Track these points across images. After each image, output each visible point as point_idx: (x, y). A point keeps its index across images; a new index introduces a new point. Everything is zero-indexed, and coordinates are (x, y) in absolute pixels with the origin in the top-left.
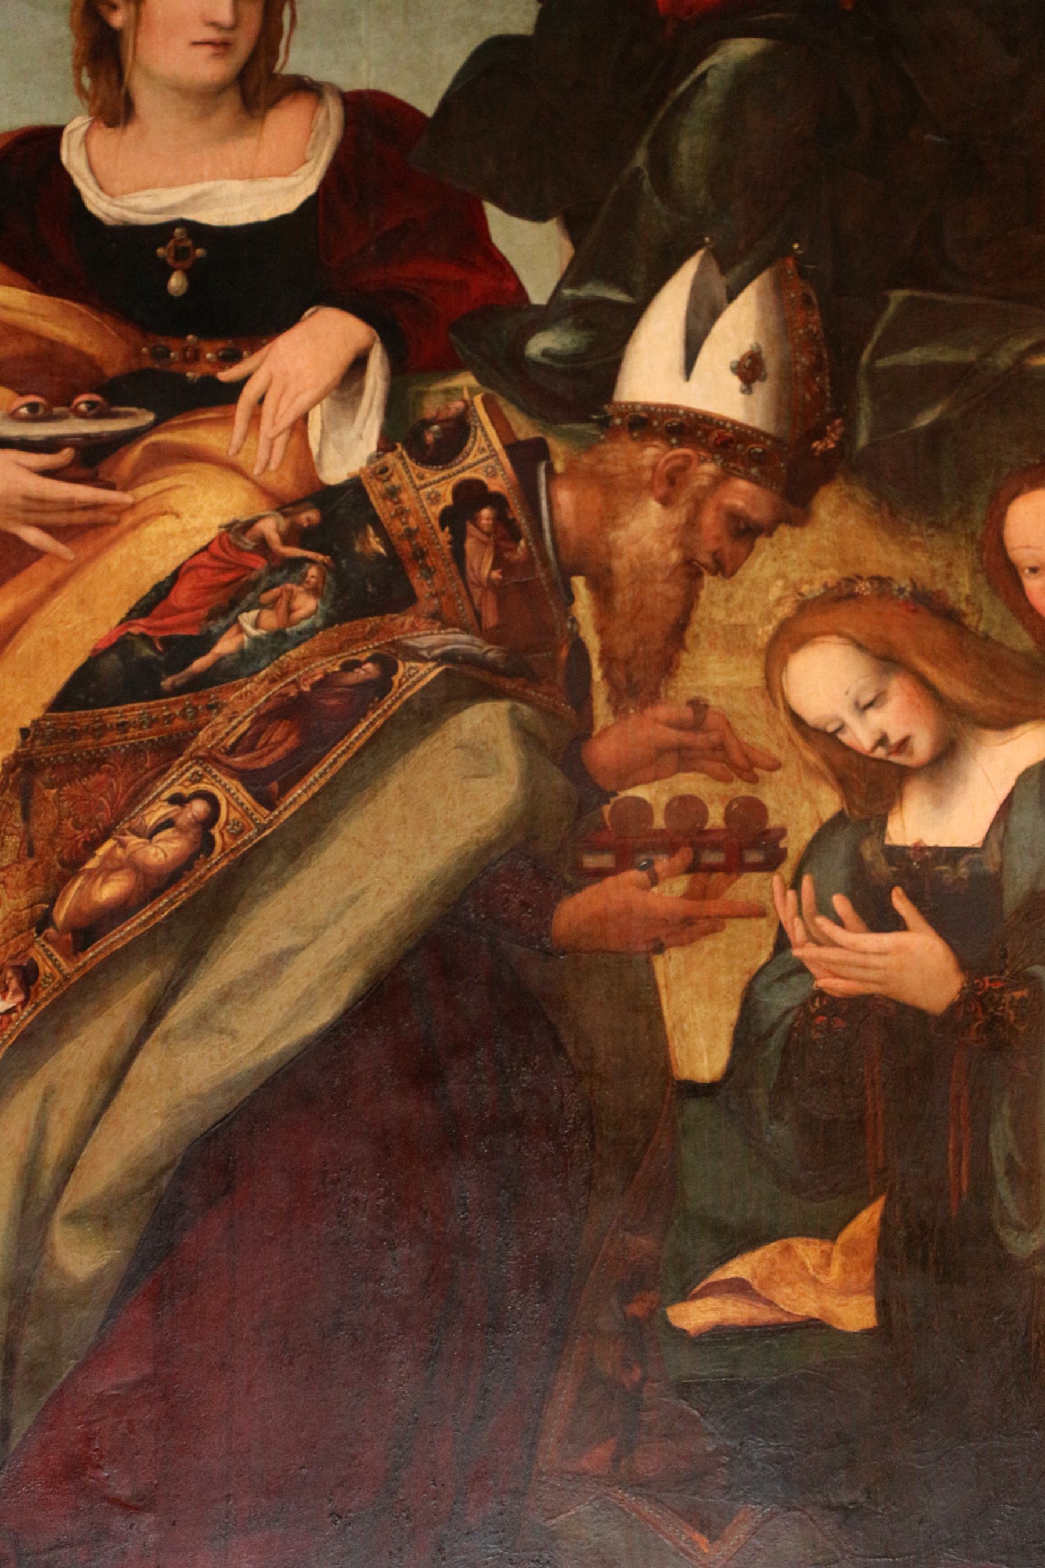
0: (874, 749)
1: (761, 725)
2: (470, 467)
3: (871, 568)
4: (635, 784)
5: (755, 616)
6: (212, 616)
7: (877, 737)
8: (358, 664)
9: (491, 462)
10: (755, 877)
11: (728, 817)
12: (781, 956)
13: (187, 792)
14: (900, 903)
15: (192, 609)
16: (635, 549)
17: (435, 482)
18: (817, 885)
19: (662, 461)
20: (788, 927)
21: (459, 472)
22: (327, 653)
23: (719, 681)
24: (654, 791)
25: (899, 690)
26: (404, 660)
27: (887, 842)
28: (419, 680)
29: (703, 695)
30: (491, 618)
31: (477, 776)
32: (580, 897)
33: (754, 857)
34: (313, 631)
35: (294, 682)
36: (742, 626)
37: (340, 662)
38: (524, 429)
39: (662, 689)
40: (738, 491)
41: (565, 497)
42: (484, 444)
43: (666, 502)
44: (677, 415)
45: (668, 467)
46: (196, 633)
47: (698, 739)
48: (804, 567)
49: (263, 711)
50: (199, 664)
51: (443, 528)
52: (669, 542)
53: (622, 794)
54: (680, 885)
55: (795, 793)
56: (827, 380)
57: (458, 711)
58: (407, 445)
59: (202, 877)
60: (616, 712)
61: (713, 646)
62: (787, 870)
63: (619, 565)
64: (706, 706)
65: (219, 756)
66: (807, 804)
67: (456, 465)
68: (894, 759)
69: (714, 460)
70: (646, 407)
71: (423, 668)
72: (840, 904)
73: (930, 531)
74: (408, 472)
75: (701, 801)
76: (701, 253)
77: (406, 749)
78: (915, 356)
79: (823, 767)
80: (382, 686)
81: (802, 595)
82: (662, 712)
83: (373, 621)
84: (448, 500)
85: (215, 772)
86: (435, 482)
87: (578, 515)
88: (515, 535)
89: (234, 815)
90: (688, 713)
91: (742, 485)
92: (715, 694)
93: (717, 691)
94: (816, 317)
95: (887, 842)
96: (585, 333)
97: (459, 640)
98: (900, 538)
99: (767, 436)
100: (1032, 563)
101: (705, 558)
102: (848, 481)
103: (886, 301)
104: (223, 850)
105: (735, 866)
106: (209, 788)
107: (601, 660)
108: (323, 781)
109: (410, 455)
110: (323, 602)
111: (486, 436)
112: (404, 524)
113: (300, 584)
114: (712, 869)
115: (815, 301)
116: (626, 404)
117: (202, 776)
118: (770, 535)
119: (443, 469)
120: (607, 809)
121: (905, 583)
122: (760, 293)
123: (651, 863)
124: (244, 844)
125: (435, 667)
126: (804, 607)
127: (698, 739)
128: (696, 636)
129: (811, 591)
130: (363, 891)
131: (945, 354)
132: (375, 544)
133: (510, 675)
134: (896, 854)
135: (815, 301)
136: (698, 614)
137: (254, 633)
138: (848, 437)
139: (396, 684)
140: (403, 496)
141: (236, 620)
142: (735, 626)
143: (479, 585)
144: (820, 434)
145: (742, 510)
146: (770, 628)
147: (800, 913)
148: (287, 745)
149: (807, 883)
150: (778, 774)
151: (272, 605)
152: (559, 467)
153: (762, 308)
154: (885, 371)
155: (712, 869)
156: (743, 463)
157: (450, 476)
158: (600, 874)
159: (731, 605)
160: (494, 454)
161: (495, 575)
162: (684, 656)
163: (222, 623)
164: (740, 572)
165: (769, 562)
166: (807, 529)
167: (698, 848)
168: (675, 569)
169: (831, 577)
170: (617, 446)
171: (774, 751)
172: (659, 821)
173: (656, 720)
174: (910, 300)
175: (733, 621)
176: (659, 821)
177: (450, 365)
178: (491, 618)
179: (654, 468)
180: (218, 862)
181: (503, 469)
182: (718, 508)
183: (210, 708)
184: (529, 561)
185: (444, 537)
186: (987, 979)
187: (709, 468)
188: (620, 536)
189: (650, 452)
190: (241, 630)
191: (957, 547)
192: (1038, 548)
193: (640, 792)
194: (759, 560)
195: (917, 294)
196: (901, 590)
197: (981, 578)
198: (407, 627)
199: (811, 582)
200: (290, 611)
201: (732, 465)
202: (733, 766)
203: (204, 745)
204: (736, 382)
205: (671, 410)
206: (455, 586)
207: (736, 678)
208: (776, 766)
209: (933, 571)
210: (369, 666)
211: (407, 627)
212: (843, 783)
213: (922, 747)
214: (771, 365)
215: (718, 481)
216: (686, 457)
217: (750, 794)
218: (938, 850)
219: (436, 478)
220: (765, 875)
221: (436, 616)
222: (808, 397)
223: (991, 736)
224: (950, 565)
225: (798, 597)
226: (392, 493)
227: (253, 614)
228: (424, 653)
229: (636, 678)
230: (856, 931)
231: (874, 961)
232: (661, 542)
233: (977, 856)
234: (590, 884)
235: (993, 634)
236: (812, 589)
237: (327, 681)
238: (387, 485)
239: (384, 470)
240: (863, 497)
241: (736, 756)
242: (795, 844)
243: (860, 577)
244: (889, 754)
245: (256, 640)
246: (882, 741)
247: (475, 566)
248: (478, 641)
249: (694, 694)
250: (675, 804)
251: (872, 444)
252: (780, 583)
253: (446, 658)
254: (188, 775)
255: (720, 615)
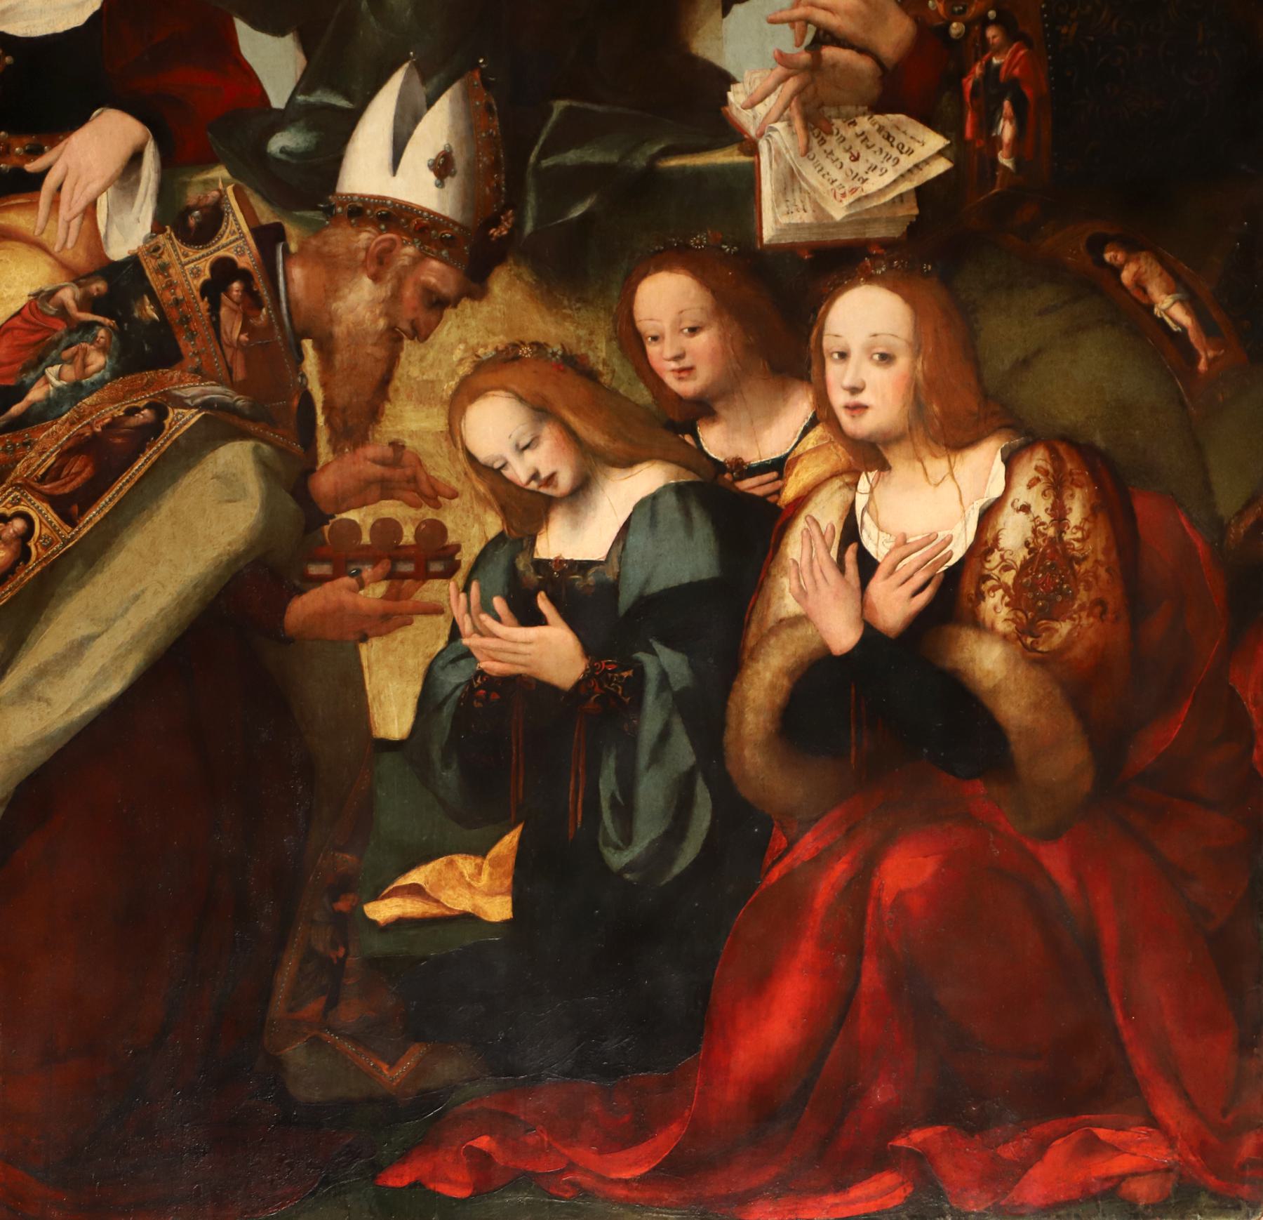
0: (528, 482)
1: (444, 462)
2: (223, 247)
3: (532, 335)
4: (348, 509)
5: (442, 374)
6: (26, 370)
7: (531, 472)
8: (138, 410)
9: (240, 242)
10: (437, 583)
11: (417, 535)
12: (453, 644)
13: (9, 512)
14: (543, 604)
15: (11, 363)
16: (351, 317)
17: (197, 260)
18: (482, 589)
19: (373, 244)
20: (459, 622)
21: (215, 251)
22: (114, 401)
23: (414, 426)
24: (362, 514)
25: (549, 436)
26: (173, 408)
27: (536, 556)
28: (185, 423)
29: (401, 438)
30: (239, 374)
31: (230, 501)
32: (305, 598)
33: (436, 567)
34: (102, 383)
35: (88, 424)
36: (432, 382)
37: (124, 408)
38: (266, 215)
39: (370, 433)
40: (431, 270)
41: (297, 273)
42: (235, 228)
43: (376, 278)
44: (384, 205)
45: (379, 247)
46: (12, 384)
47: (397, 473)
48: (481, 333)
49: (65, 447)
50: (16, 409)
51: (203, 298)
52: (378, 312)
53: (338, 517)
54: (380, 589)
55: (468, 516)
56: (503, 177)
57: (215, 448)
58: (174, 228)
59: (22, 579)
60: (334, 451)
61: (409, 397)
62: (460, 577)
63: (339, 330)
64: (403, 447)
65: (33, 483)
66: (476, 526)
67: (213, 245)
68: (543, 490)
69: (413, 244)
70: (362, 197)
71: (188, 413)
72: (499, 604)
73: (578, 305)
74: (175, 251)
75: (397, 523)
76: (406, 65)
77: (174, 479)
78: (572, 157)
79: (490, 497)
80: (156, 428)
81: (478, 356)
82: (371, 451)
83: (149, 375)
84: (207, 275)
85: (30, 497)
86: (197, 260)
87: (307, 287)
88: (259, 305)
89: (45, 531)
90: (389, 452)
91: (435, 264)
92: (410, 436)
93: (412, 434)
94: (497, 123)
95: (536, 556)
96: (315, 134)
97: (215, 391)
98: (554, 311)
99: (455, 223)
100: (653, 333)
101: (405, 326)
102: (517, 264)
103: (550, 110)
104: (37, 559)
105: (423, 575)
106: (26, 509)
107: (324, 408)
108: (112, 505)
109: (177, 236)
110: (110, 358)
111: (236, 220)
112: (173, 294)
113: (92, 344)
114: (405, 576)
115: (495, 108)
116: (347, 195)
117: (20, 500)
118: (455, 306)
119: (202, 249)
120: (327, 528)
121: (557, 348)
122: (451, 101)
123: (359, 572)
124: (53, 554)
125: (197, 413)
126: (480, 366)
127: (397, 473)
128: (397, 390)
129: (485, 354)
130: (143, 592)
131: (592, 155)
132: (150, 312)
133: (254, 420)
134: (542, 565)
135: (495, 108)
136: (399, 372)
137: (58, 383)
138: (518, 225)
139: (167, 426)
140: (172, 271)
141: (43, 373)
142: (427, 382)
143: (231, 345)
144: (496, 223)
145: (435, 285)
146: (453, 384)
147: (469, 611)
148: (84, 475)
149: (474, 588)
150: (456, 501)
151: (71, 361)
152: (293, 247)
153: (454, 115)
154: (548, 169)
155: (405, 576)
156: (436, 247)
157: (208, 255)
158: (321, 580)
159: (424, 364)
160: (243, 236)
161: (244, 337)
162: (388, 406)
163: (32, 375)
164: (431, 337)
165: (454, 329)
166: (484, 303)
167: (395, 560)
168: (381, 334)
169: (501, 342)
170: (339, 231)
171: (454, 483)
172: (366, 539)
173: (366, 459)
174: (568, 110)
175: (425, 377)
176: (366, 539)
177: (210, 161)
178: (239, 374)
179: (367, 249)
180: (33, 567)
181: (249, 249)
182: (415, 284)
183: (25, 445)
184: (270, 326)
185: (204, 305)
186: (603, 662)
187: (410, 250)
188: (339, 307)
189: (364, 236)
190: (47, 382)
191: (598, 318)
192: (658, 321)
193: (353, 515)
194: (446, 328)
195: (575, 104)
196: (554, 354)
197: (614, 344)
198: (175, 379)
199: (485, 346)
200: (85, 366)
201: (427, 247)
202: (423, 495)
203: (21, 475)
204: (431, 177)
205: (381, 201)
206: (213, 347)
207: (426, 424)
208: (454, 495)
209: (579, 339)
210: (146, 412)
211: (175, 379)
212: (505, 511)
213: (565, 481)
214: (460, 162)
215: (417, 261)
216: (391, 239)
217: (435, 517)
218: (573, 563)
219: (197, 256)
220: (444, 581)
221: (197, 371)
222: (487, 190)
223: (616, 473)
224: (591, 333)
225: (475, 359)
226: (163, 269)
227: (56, 368)
228: (189, 402)
229: (350, 424)
230: (510, 626)
231: (522, 648)
232: (372, 312)
233: (601, 567)
234: (314, 587)
235: (621, 391)
236: (486, 352)
237: (115, 423)
238: (159, 261)
239: (157, 249)
240: (528, 277)
241: (425, 488)
242: (467, 557)
243: (523, 343)
244: (540, 486)
245: (58, 389)
246: (535, 476)
247: (228, 330)
248: (230, 392)
249: (394, 437)
250: (378, 525)
251: (535, 232)
252: (462, 347)
253: (205, 405)
254: (10, 499)
255: (415, 372)
